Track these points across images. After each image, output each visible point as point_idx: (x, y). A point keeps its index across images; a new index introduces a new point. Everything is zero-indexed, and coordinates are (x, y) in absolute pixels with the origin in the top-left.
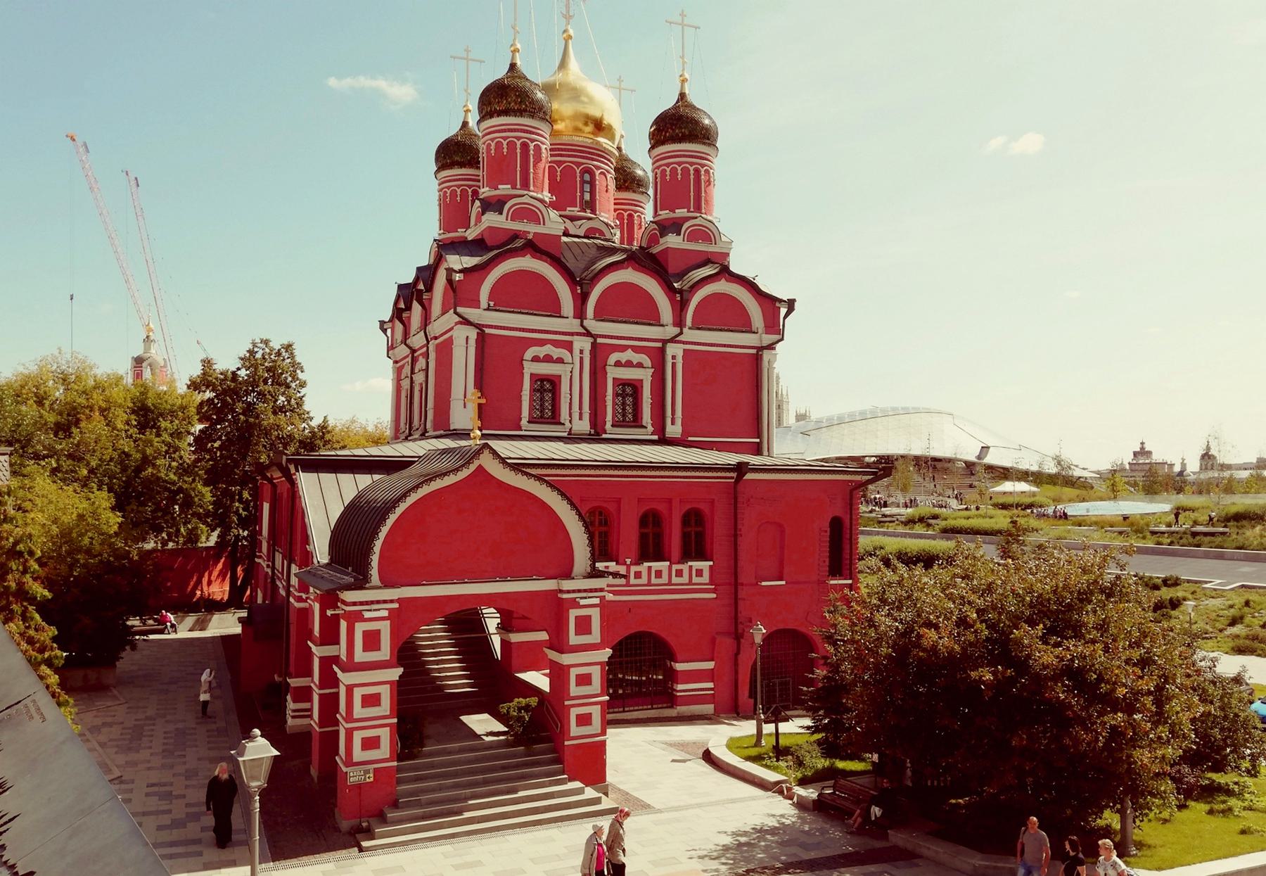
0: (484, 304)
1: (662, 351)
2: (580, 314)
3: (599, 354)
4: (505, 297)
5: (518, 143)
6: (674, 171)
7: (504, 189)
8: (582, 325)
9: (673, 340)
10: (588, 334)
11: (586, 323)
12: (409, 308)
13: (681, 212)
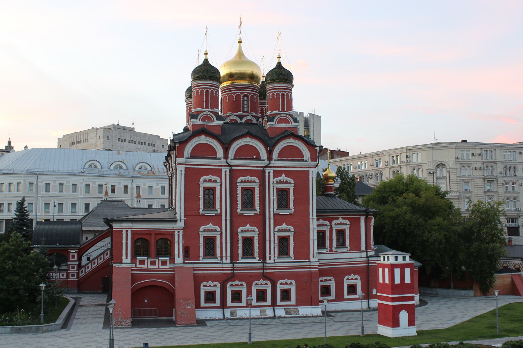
1: (264, 171)
2: (226, 157)
3: (234, 174)
4: (195, 154)
8: (227, 163)
10: (229, 165)
11: (229, 161)
13: (277, 112)
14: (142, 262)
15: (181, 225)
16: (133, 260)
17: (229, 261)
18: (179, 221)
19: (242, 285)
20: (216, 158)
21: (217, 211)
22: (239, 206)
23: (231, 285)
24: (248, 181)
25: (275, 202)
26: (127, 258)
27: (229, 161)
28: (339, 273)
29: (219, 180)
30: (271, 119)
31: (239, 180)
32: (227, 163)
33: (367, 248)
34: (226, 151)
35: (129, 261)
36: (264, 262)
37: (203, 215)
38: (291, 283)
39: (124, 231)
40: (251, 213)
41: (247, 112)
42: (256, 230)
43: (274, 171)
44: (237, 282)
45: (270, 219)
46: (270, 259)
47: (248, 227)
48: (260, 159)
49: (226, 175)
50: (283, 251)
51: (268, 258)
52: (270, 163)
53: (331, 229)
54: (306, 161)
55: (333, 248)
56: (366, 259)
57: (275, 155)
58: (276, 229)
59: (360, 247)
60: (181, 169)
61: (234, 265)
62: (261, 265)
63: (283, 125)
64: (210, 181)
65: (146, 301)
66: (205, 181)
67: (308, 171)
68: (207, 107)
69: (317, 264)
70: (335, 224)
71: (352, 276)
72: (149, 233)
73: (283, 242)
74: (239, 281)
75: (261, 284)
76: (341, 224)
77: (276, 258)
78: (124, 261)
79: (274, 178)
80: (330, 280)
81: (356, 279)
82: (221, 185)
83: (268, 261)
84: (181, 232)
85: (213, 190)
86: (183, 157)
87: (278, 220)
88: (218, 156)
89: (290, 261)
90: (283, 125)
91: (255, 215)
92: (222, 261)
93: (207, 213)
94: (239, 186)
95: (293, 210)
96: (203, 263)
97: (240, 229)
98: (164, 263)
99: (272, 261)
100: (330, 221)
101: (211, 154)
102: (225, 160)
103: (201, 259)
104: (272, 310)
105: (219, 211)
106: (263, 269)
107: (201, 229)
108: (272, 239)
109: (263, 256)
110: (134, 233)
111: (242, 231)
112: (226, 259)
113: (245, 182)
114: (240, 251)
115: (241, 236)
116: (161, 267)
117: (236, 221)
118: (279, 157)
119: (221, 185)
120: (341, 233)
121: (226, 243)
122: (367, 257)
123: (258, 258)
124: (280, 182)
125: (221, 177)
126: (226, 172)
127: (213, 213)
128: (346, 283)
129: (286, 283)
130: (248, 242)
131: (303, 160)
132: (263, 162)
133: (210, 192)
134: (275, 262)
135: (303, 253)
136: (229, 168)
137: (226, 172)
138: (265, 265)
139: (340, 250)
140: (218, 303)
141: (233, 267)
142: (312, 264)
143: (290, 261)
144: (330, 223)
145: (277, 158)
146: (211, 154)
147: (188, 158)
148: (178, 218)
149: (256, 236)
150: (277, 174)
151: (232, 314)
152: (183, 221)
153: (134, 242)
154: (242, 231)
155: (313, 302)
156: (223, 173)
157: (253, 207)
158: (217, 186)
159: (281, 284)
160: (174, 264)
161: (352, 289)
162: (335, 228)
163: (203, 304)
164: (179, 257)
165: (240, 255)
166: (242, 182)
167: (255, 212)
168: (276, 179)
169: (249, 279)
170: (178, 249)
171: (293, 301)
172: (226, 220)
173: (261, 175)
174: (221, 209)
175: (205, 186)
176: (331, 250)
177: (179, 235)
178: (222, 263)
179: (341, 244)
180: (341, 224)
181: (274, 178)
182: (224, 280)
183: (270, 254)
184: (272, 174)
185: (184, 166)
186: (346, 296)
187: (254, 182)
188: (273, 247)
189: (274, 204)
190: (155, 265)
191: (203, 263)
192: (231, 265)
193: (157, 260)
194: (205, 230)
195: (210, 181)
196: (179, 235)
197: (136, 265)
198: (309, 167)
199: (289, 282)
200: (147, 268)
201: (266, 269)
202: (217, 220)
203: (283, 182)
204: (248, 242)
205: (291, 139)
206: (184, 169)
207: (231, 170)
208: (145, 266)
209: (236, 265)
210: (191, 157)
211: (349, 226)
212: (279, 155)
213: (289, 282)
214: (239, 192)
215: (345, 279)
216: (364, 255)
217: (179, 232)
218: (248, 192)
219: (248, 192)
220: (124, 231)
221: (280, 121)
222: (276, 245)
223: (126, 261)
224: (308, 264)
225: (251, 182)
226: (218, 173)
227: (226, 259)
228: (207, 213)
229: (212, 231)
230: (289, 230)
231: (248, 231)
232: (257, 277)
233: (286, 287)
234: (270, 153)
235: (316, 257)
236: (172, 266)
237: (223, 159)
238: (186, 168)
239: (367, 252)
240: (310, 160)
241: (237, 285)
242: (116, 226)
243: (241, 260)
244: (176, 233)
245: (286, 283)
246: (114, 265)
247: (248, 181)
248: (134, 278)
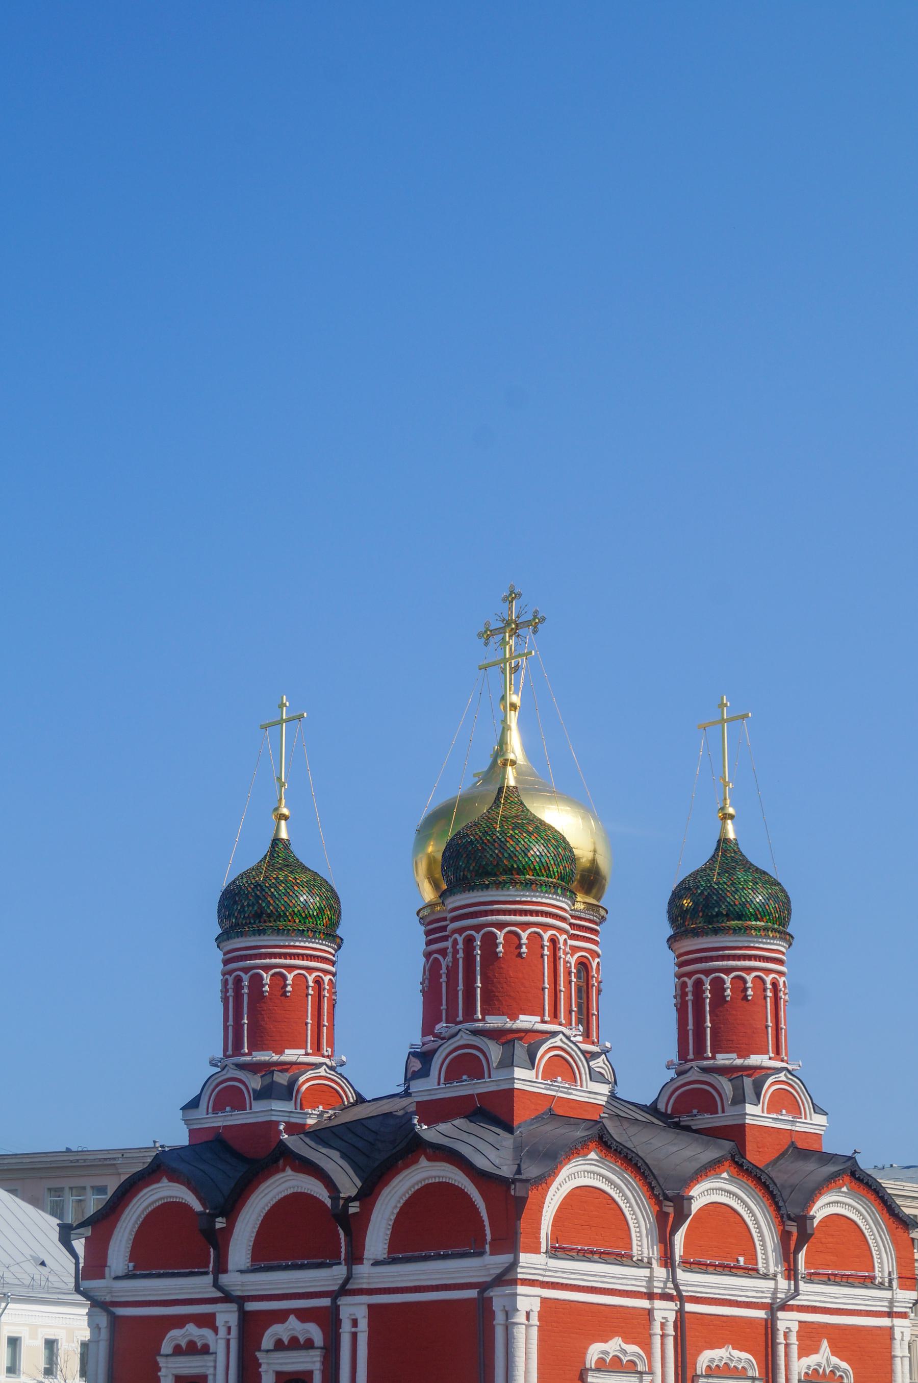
1: (770, 1327)
11: (681, 1275)
20: (623, 1258)
54: (881, 1286)
79: (799, 1358)
86: (537, 1251)
125: (647, 1346)
131: (868, 1282)
156: (657, 1329)
184: (793, 1339)
198: (890, 1314)
206: (536, 1305)
210: (555, 1252)
226: (635, 1326)
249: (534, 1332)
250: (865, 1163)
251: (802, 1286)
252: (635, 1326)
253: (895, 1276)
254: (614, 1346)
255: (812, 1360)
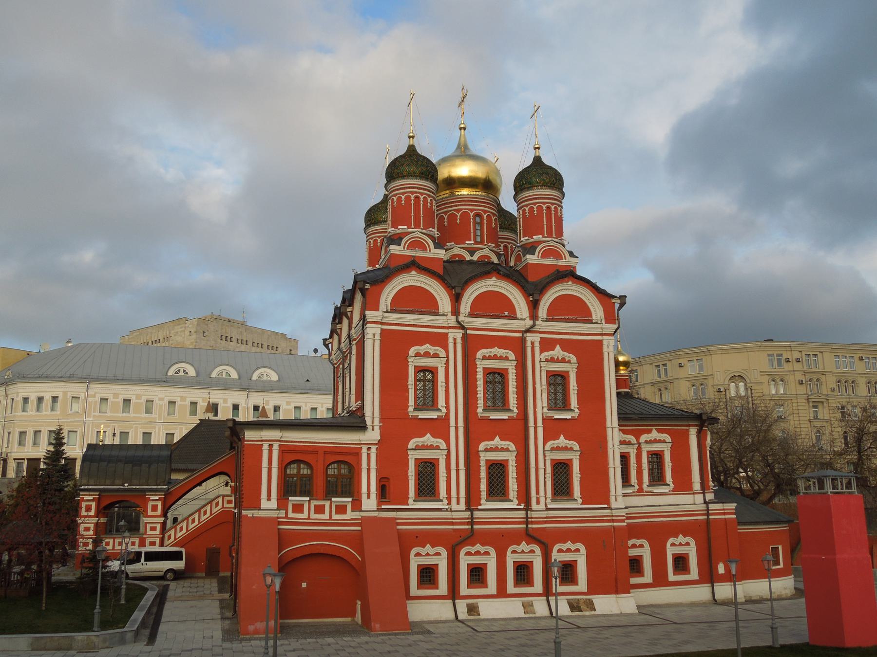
0: (382, 307)
1: (523, 340)
2: (456, 312)
3: (472, 344)
4: (397, 306)
5: (413, 197)
6: (531, 209)
7: (402, 228)
8: (458, 322)
9: (528, 331)
11: (461, 318)
12: (340, 322)
13: (537, 238)
14: (298, 508)
15: (373, 435)
16: (282, 503)
17: (462, 506)
18: (370, 427)
19: (487, 553)
21: (440, 410)
22: (481, 402)
23: (468, 554)
24: (495, 358)
25: (545, 396)
26: (269, 499)
27: (461, 318)
28: (657, 532)
29: (442, 353)
30: (530, 249)
31: (479, 354)
32: (458, 322)
33: (704, 488)
34: (456, 299)
35: (273, 504)
36: (528, 508)
37: (415, 418)
38: (578, 550)
39: (266, 446)
40: (504, 416)
41: (482, 243)
42: (512, 447)
43: (542, 340)
44: (478, 547)
45: (536, 428)
46: (538, 503)
47: (497, 442)
48: (515, 318)
49: (455, 344)
50: (562, 488)
51: (534, 501)
52: (534, 325)
53: (639, 450)
54: (597, 323)
55: (645, 486)
56: (704, 507)
57: (543, 311)
58: (548, 447)
59: (691, 484)
60: (373, 332)
61: (472, 514)
62: (522, 514)
63: (551, 261)
64: (427, 355)
65: (304, 585)
66: (418, 355)
67: (601, 342)
68: (417, 226)
69: (623, 512)
70: (646, 442)
71: (681, 539)
72: (312, 450)
73: (561, 469)
74: (483, 545)
75: (523, 552)
76: (655, 441)
77: (549, 501)
78: (264, 504)
79: (541, 352)
80: (641, 546)
81: (688, 544)
82: (447, 363)
83: (534, 506)
84: (374, 450)
85: (432, 372)
86: (378, 310)
87: (552, 429)
88: (441, 311)
89: (575, 509)
90: (551, 261)
91: (510, 419)
92: (450, 507)
93: (423, 415)
94: (481, 365)
95: (577, 411)
96: (415, 511)
97: (482, 446)
98: (341, 509)
99: (542, 506)
100: (637, 436)
101: (428, 305)
102: (454, 318)
103: (411, 501)
104: (545, 603)
105: (444, 410)
106: (527, 523)
107: (412, 444)
108: (541, 465)
109: (525, 497)
110: (283, 451)
111: (486, 450)
112: (458, 503)
113: (490, 358)
114: (483, 487)
115: (484, 457)
116: (335, 516)
117: (476, 430)
118: (548, 314)
119: (447, 363)
120: (656, 458)
121: (458, 471)
122: (705, 502)
123: (516, 501)
124: (552, 360)
126: (455, 339)
127: (434, 415)
128: (670, 551)
129: (569, 550)
130: (497, 470)
131: (590, 321)
132: (522, 322)
133: (427, 374)
134: (548, 509)
135: (597, 492)
136: (461, 331)
137: (455, 339)
138: (532, 514)
139: (657, 490)
140: (443, 587)
141: (472, 518)
142: (615, 513)
143: (575, 509)
144: (638, 439)
145: (545, 316)
146: (428, 305)
147: (387, 312)
148: (369, 421)
149: (511, 458)
150: (547, 345)
151: (472, 609)
152: (377, 429)
153: (283, 468)
154: (486, 450)
155: (620, 587)
156: (451, 340)
157: (505, 407)
158: (439, 364)
159: (560, 551)
160: (361, 511)
161: (681, 563)
162: (646, 448)
163: (414, 590)
164: (369, 497)
165: (484, 495)
166: (484, 358)
167: (510, 414)
168: (545, 354)
169: (501, 541)
170: (368, 481)
171: (582, 583)
172: (457, 428)
173: (518, 346)
174: (447, 408)
175: (417, 364)
176: (641, 490)
177: (369, 455)
178: (451, 511)
179: (657, 477)
180: (655, 441)
181: (541, 352)
182: (454, 542)
183: (538, 492)
184: (537, 344)
185: (379, 326)
186: (672, 577)
187: (507, 359)
188: (542, 481)
189: (542, 401)
190: (323, 512)
191: (415, 511)
192: (467, 514)
193: (327, 504)
194: (419, 448)
195: (427, 355)
196: (369, 455)
197: (287, 513)
199: (573, 547)
200: (309, 518)
201: (532, 523)
202: (440, 427)
203: (558, 361)
204: (497, 470)
205: (570, 283)
206: (379, 331)
207: (465, 337)
208: (305, 515)
209: (477, 514)
210: (393, 311)
211: (670, 445)
212: (549, 312)
213: (573, 547)
214: (480, 376)
215: (668, 545)
216: (699, 498)
217: (369, 449)
218: (496, 377)
219: (496, 377)
220: (266, 446)
221: (546, 254)
222: (549, 475)
223: (269, 505)
224: (607, 512)
225: (501, 358)
226: (440, 340)
227: (458, 503)
228: (423, 415)
229: (431, 448)
230: (571, 449)
231: (496, 449)
232: (514, 538)
233: (568, 557)
234: (534, 306)
235: (621, 501)
236: (357, 515)
237: (450, 314)
238: (382, 329)
239: (704, 493)
240: (603, 321)
241: (478, 553)
242: (250, 435)
243: (485, 505)
244: (364, 450)
245: (569, 550)
246: (244, 513)
247: (495, 358)
248: (283, 538)
249: (377, 343)
250: (579, 273)
251: (538, 322)
252: (440, 340)
253: (603, 317)
254: (427, 347)
255: (549, 354)
